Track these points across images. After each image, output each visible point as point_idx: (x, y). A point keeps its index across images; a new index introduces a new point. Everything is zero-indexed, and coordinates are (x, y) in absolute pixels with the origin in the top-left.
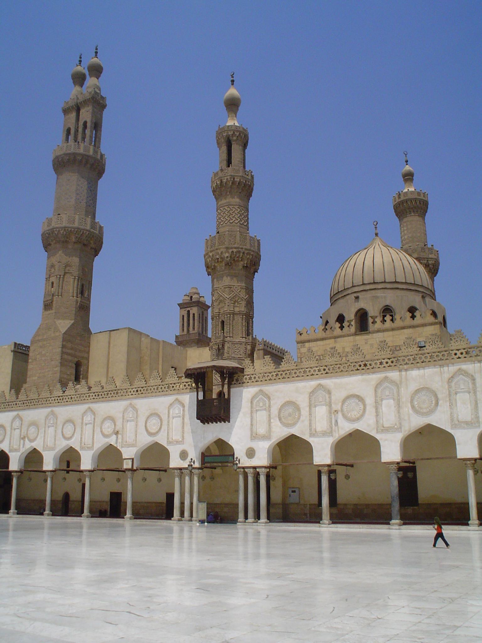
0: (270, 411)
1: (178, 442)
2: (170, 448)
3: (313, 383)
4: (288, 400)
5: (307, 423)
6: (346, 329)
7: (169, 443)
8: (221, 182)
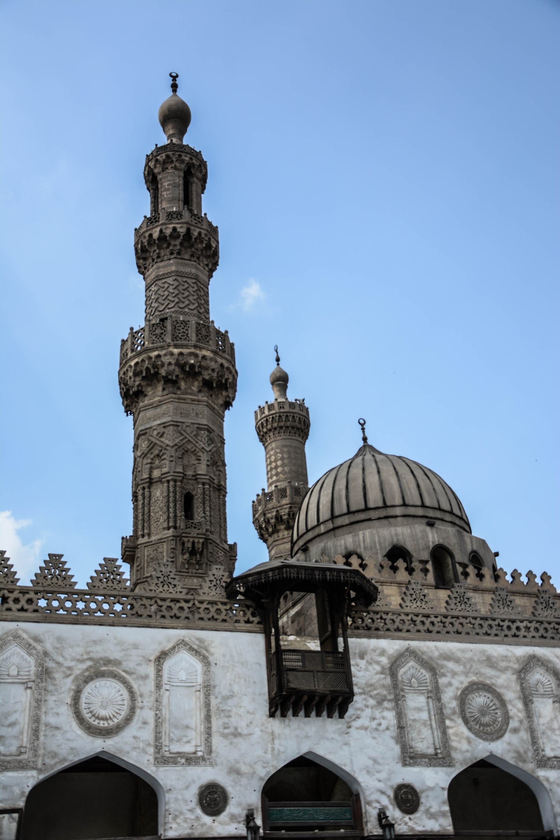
0: (439, 700)
1: (191, 760)
2: (166, 777)
3: (521, 651)
4: (474, 678)
5: (524, 735)
6: (418, 575)
7: (163, 760)
8: (188, 230)
